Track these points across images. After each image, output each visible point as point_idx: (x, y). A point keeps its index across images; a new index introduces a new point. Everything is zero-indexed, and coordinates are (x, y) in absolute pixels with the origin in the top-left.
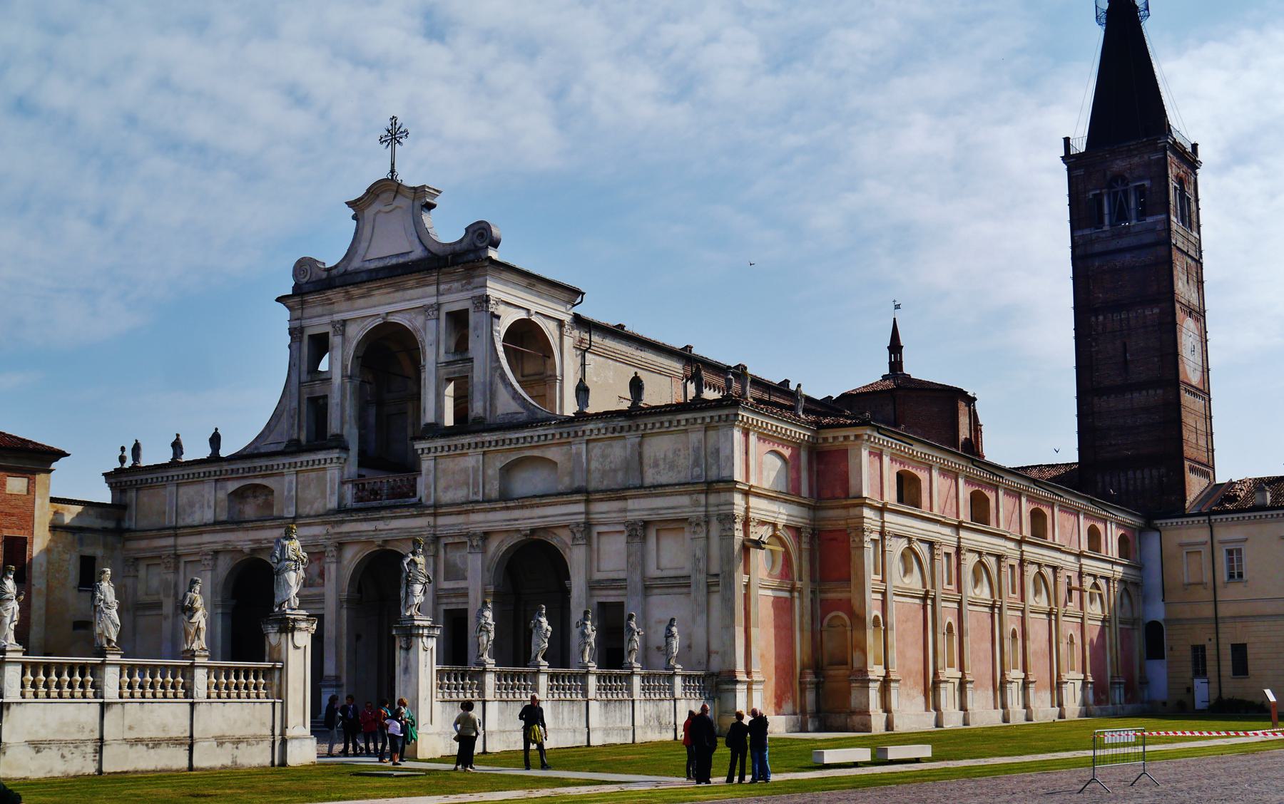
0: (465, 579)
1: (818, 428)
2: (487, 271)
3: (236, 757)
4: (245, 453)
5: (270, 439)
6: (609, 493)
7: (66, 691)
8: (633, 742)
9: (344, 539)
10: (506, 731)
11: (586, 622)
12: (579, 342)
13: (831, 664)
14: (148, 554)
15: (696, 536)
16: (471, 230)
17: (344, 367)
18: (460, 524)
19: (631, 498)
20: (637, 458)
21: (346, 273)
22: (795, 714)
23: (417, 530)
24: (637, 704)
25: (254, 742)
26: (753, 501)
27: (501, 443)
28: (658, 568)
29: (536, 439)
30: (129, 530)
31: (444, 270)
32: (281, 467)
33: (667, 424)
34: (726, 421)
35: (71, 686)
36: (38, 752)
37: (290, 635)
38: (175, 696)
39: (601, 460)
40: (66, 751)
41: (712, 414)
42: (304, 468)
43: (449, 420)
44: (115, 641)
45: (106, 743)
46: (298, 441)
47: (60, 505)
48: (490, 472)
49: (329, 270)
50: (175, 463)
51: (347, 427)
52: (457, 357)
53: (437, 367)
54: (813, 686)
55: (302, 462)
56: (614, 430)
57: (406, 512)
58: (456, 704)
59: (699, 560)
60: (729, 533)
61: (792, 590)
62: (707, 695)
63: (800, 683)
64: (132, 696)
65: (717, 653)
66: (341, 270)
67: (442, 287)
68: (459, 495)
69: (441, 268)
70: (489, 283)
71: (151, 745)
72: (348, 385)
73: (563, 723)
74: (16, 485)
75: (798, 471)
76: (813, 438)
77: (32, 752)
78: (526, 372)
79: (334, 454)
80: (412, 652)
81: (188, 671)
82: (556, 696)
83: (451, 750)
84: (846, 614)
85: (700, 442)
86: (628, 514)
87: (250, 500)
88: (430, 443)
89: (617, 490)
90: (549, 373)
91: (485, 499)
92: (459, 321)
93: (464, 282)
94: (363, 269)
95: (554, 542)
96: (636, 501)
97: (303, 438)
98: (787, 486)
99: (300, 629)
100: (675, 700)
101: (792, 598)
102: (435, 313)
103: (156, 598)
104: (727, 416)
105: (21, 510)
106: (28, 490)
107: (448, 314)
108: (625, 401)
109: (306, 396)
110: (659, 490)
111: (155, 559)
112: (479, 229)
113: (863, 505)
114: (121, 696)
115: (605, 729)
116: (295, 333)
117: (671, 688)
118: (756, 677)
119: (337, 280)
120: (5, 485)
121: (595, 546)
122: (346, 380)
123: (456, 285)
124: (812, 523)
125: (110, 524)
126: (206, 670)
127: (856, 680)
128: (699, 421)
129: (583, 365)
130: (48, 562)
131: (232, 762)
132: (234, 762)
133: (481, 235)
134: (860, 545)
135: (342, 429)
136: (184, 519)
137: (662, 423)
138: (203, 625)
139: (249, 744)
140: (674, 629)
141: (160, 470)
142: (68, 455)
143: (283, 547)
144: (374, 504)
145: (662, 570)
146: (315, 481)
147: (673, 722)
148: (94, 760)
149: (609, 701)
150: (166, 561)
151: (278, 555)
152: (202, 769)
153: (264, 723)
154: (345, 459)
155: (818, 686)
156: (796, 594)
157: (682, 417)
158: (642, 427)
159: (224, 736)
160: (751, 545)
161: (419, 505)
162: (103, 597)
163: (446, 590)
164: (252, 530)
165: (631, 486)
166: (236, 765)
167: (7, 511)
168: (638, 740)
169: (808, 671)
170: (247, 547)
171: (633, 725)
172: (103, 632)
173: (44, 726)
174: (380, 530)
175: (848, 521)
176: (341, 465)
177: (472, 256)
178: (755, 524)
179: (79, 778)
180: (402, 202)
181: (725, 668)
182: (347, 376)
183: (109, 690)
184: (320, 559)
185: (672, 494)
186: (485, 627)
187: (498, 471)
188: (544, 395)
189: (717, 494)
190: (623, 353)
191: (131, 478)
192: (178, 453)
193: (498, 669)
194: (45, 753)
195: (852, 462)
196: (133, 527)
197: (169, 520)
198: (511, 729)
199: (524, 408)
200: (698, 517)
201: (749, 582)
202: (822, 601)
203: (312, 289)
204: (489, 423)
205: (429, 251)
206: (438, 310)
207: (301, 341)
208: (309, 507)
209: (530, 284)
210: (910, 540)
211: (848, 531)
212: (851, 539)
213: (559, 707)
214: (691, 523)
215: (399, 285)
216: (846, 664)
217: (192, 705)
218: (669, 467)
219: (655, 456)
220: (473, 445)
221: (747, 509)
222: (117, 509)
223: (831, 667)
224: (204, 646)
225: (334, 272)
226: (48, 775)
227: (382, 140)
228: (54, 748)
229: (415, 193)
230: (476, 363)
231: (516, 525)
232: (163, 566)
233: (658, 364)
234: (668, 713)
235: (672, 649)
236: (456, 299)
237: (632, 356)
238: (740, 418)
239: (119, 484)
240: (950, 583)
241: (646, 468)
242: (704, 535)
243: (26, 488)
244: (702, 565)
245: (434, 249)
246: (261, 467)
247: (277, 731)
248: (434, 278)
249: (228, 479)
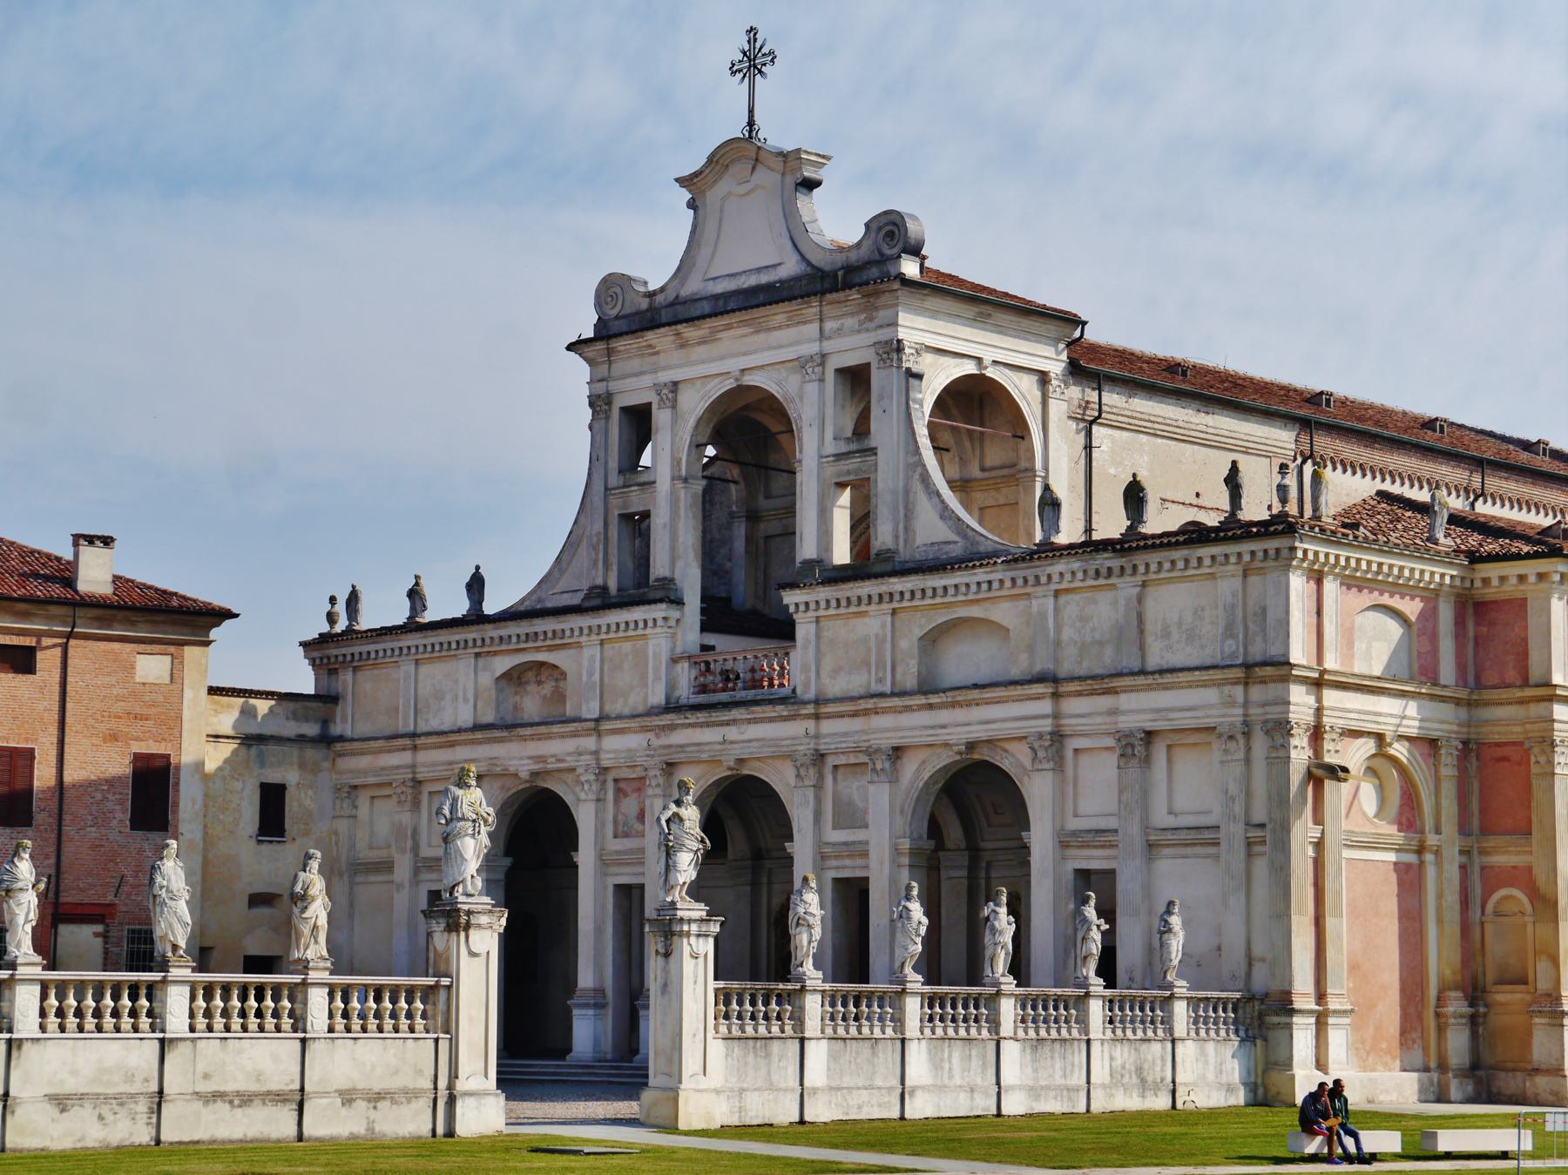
0: (866, 826)
1: (1471, 562)
2: (897, 298)
3: (373, 1122)
4: (522, 608)
5: (561, 586)
6: (1089, 682)
7: (108, 1021)
8: (1088, 1111)
9: (676, 756)
10: (843, 1088)
11: (998, 909)
12: (1080, 406)
13: (1502, 981)
14: (372, 780)
15: (1229, 758)
16: (874, 226)
17: (676, 462)
18: (857, 732)
19: (1125, 691)
20: (1135, 623)
21: (677, 302)
22: (1426, 1069)
23: (788, 742)
24: (1095, 1047)
25: (404, 1100)
26: (1331, 697)
27: (918, 595)
28: (1170, 812)
29: (974, 588)
30: (341, 739)
31: (829, 297)
32: (576, 633)
33: (1181, 565)
34: (1276, 559)
35: (116, 1014)
36: (63, 1111)
37: (463, 934)
38: (278, 1029)
39: (1078, 624)
40: (105, 1111)
41: (1253, 548)
42: (612, 635)
43: (841, 554)
44: (184, 946)
45: (168, 1098)
46: (605, 588)
47: (226, 698)
48: (904, 644)
49: (651, 295)
50: (412, 626)
51: (680, 564)
52: (854, 447)
53: (820, 464)
54: (1464, 1021)
55: (608, 625)
56: (1097, 573)
57: (768, 711)
58: (751, 1042)
59: (1233, 799)
60: (1282, 754)
61: (1420, 850)
62: (1242, 1033)
63: (1437, 1015)
64: (210, 1029)
65: (1263, 960)
66: (670, 295)
67: (829, 325)
68: (854, 682)
69: (823, 293)
70: (904, 318)
71: (236, 1102)
72: (682, 494)
73: (951, 1077)
74: (151, 667)
75: (1434, 637)
76: (1463, 579)
77: (53, 1111)
78: (988, 463)
79: (658, 611)
80: (672, 959)
81: (297, 993)
82: (939, 1032)
83: (740, 1117)
84: (1521, 890)
85: (1234, 595)
86: (1122, 718)
87: (531, 688)
88: (809, 594)
89: (1101, 677)
90: (1023, 464)
91: (896, 691)
92: (856, 379)
93: (863, 316)
94: (704, 294)
95: (1006, 765)
96: (1134, 696)
97: (613, 585)
98: (1410, 666)
99: (479, 926)
100: (1173, 1041)
101: (1422, 863)
102: (816, 370)
103: (384, 853)
104: (1278, 551)
105: (160, 709)
106: (172, 674)
107: (840, 372)
108: (1174, 506)
109: (616, 513)
110: (1169, 678)
111: (381, 788)
112: (887, 224)
113: (1552, 699)
114: (192, 1029)
115: (1032, 1089)
116: (599, 403)
117: (1168, 1022)
118: (1333, 1004)
119: (663, 312)
120: (133, 667)
121: (1070, 772)
122: (680, 485)
123: (850, 322)
124: (1465, 730)
125: (312, 730)
126: (327, 990)
127: (1540, 1012)
128: (1233, 559)
129: (1089, 448)
130: (206, 795)
131: (367, 1130)
132: (370, 1129)
133: (890, 235)
134: (1548, 770)
135: (673, 572)
136: (427, 720)
137: (1173, 562)
138: (323, 921)
139: (394, 1102)
140: (1175, 921)
141: (388, 638)
142: (236, 616)
143: (455, 800)
144: (723, 697)
145: (1176, 815)
146: (630, 658)
147: (1169, 1078)
148: (148, 1124)
149: (1040, 1040)
150: (399, 791)
151: (446, 811)
152: (318, 1139)
153: (421, 1071)
154: (678, 621)
155: (1474, 1021)
156: (1429, 857)
157: (1206, 552)
158: (1142, 569)
159: (354, 1089)
160: (1324, 774)
161: (790, 699)
162: (165, 883)
163: (834, 844)
164: (533, 739)
165: (1125, 671)
166: (373, 1133)
167: (138, 710)
168: (1097, 1107)
169: (1453, 994)
170: (524, 769)
171: (1088, 1082)
172: (166, 934)
173: (74, 1073)
174: (732, 742)
175: (1528, 727)
176: (670, 631)
177: (874, 272)
178: (1335, 736)
179: (124, 1153)
180: (766, 178)
181: (1275, 986)
182: (680, 478)
183: (174, 1020)
184: (639, 790)
185: (1190, 685)
186: (805, 919)
187: (916, 644)
188: (1017, 503)
189: (1264, 686)
190: (1168, 422)
191: (344, 651)
192: (418, 608)
193: (827, 986)
194: (75, 1112)
195: (1533, 621)
196: (348, 733)
197: (405, 724)
198: (852, 1085)
199: (959, 534)
200: (1232, 724)
201: (1322, 839)
202: (1483, 868)
203: (625, 329)
204: (902, 559)
205: (809, 263)
206: (822, 364)
207: (607, 418)
208: (621, 701)
209: (981, 314)
211: (1526, 746)
212: (1533, 759)
213: (943, 1051)
214: (1220, 736)
215: (760, 323)
216: (1526, 983)
217: (303, 1041)
218: (1187, 639)
219: (1165, 619)
220: (875, 599)
221: (1319, 711)
222: (326, 699)
223: (1500, 987)
224: (325, 953)
225: (660, 299)
226: (79, 1145)
227: (735, 69)
228: (87, 1104)
229: (785, 162)
230: (882, 456)
231: (944, 735)
232: (395, 798)
233: (1242, 436)
234: (1159, 1062)
235: (1169, 953)
236: (852, 348)
237: (1186, 426)
238: (1300, 554)
239: (325, 661)
241: (1150, 640)
242: (1241, 755)
243: (169, 672)
244: (1238, 809)
245: (816, 258)
246: (545, 632)
247: (443, 1083)
248: (814, 310)
249: (495, 653)
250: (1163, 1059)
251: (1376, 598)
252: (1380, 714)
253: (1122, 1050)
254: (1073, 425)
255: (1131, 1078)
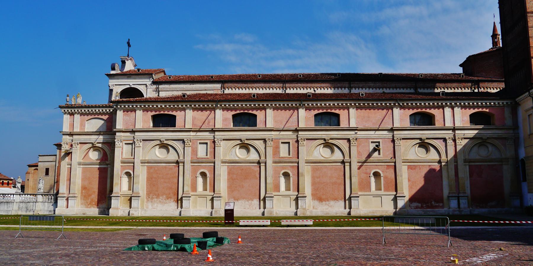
12: (155, 89)
209: (128, 77)
210: (161, 141)
233: (204, 87)
234: (32, 206)
240: (207, 155)
250: (33, 205)
251: (93, 117)
252: (91, 139)
253: (22, 204)
254: (155, 92)
255: (24, 209)
